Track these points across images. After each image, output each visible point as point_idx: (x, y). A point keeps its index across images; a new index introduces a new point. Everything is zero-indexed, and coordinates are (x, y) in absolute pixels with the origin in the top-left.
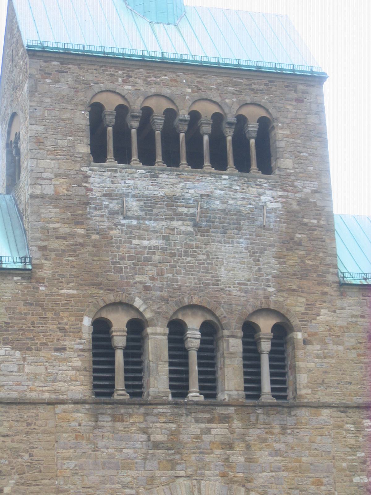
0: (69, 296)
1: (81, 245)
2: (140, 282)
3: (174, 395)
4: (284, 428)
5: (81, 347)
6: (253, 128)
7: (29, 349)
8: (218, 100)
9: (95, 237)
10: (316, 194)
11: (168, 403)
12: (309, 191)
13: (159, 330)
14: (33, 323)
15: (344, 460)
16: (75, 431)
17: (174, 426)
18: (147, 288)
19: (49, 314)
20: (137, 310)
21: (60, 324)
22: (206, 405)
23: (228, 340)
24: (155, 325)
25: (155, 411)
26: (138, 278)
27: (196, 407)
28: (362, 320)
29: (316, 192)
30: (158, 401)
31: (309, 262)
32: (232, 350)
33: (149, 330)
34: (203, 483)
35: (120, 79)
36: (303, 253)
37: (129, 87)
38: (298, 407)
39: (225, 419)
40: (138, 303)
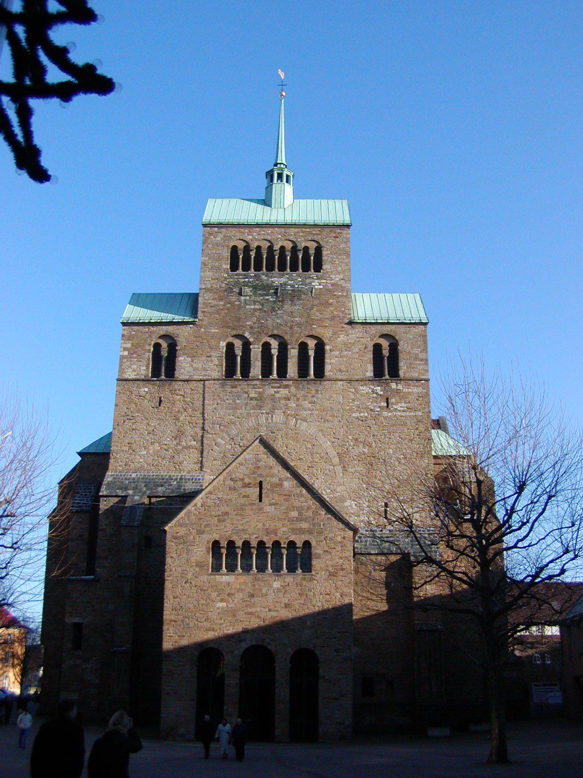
0: (215, 332)
1: (222, 309)
2: (248, 325)
3: (262, 377)
4: (317, 391)
5: (218, 355)
6: (312, 252)
7: (194, 357)
8: (294, 240)
9: (228, 306)
10: (342, 281)
11: (258, 379)
12: (338, 279)
13: (256, 346)
14: (197, 345)
15: (348, 406)
16: (213, 392)
17: (262, 390)
18: (251, 328)
19: (205, 341)
20: (246, 338)
21: (209, 345)
22: (278, 380)
23: (290, 351)
24: (254, 344)
25: (253, 383)
26: (248, 323)
27: (273, 381)
28: (362, 339)
29: (342, 279)
30: (253, 379)
31: (336, 313)
32: (292, 355)
33: (251, 347)
34: (274, 416)
35: (246, 234)
36: (332, 309)
37: (250, 237)
38: (325, 381)
39: (286, 387)
40: (247, 335)
